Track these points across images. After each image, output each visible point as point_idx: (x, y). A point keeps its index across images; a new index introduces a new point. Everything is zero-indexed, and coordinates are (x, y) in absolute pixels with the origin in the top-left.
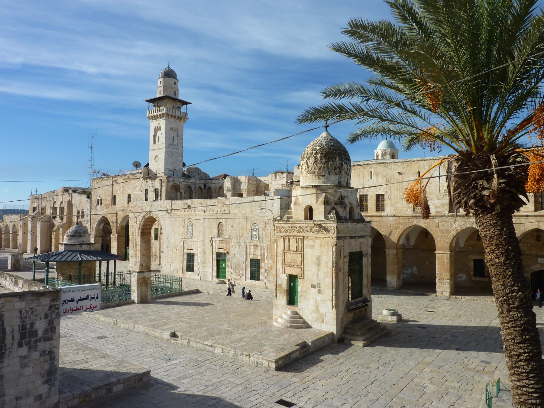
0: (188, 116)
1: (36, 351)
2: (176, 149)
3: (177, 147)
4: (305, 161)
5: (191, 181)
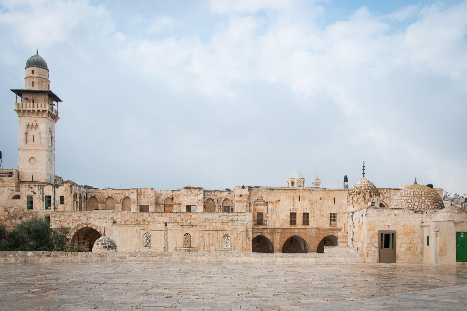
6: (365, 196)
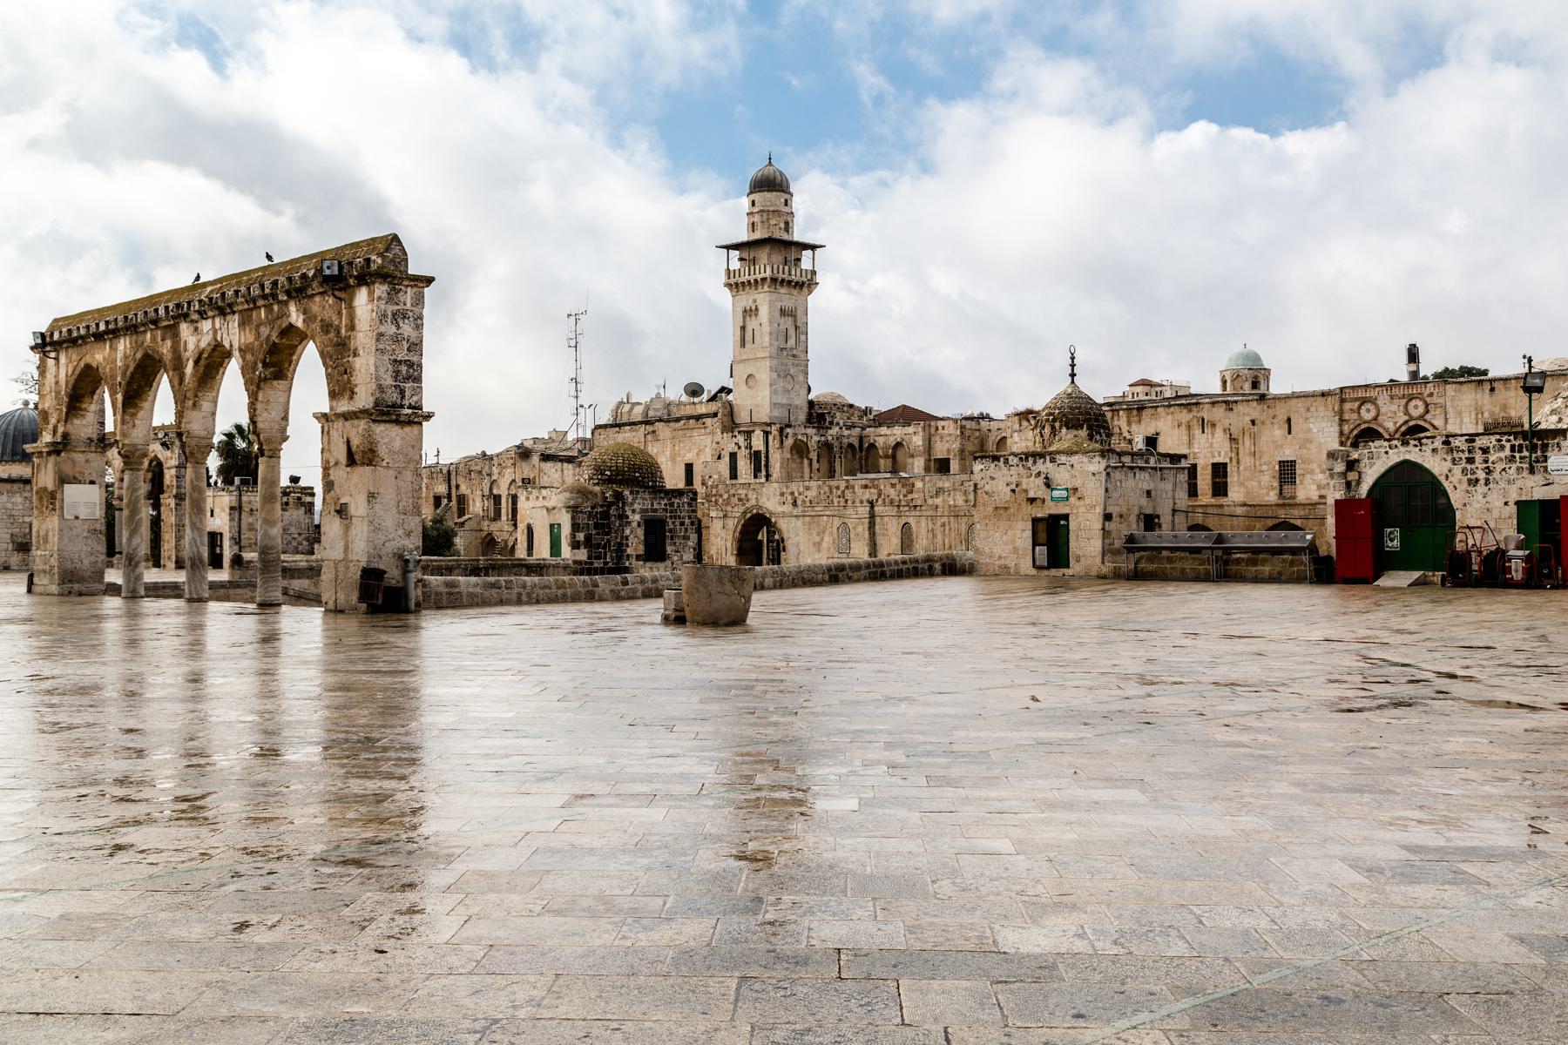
0: (818, 279)
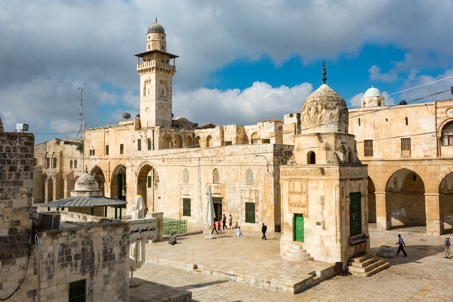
0: (176, 69)
1: (114, 271)
2: (166, 100)
3: (166, 99)
4: (306, 111)
5: (181, 131)
6: (310, 112)
